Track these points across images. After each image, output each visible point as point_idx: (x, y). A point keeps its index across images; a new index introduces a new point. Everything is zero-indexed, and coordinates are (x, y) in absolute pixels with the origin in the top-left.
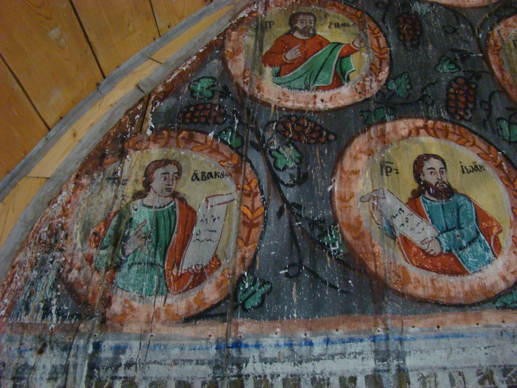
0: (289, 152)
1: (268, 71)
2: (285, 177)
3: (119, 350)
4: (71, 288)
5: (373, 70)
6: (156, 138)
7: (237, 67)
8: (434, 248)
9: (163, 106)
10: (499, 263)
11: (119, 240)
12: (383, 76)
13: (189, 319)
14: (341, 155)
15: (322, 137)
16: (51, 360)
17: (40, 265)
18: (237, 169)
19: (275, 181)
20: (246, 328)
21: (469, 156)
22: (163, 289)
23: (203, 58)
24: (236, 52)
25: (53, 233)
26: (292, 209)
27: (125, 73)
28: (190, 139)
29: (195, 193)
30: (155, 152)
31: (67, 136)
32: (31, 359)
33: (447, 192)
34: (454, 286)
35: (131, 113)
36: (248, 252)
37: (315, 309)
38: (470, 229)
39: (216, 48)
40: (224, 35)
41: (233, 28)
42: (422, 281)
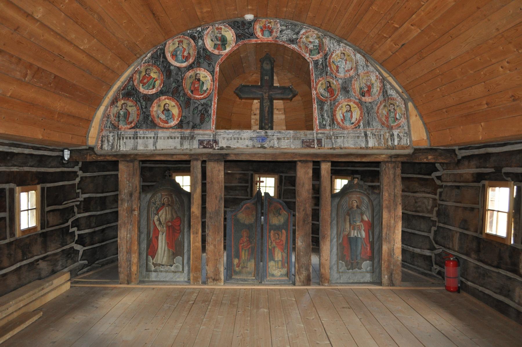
0: (144, 103)
1: (141, 85)
2: (143, 107)
3: (121, 133)
4: (113, 124)
5: (160, 85)
6: (122, 99)
7: (135, 84)
8: (164, 120)
10: (174, 122)
11: (119, 117)
13: (130, 129)
16: (111, 134)
17: (107, 121)
19: (142, 108)
20: (138, 130)
21: (173, 104)
22: (126, 124)
23: (129, 81)
24: (135, 80)
25: (108, 115)
28: (128, 99)
29: (130, 109)
31: (107, 98)
33: (168, 110)
34: (166, 125)
37: (147, 128)
38: (170, 117)
40: (133, 75)
41: (135, 73)
42: (162, 124)
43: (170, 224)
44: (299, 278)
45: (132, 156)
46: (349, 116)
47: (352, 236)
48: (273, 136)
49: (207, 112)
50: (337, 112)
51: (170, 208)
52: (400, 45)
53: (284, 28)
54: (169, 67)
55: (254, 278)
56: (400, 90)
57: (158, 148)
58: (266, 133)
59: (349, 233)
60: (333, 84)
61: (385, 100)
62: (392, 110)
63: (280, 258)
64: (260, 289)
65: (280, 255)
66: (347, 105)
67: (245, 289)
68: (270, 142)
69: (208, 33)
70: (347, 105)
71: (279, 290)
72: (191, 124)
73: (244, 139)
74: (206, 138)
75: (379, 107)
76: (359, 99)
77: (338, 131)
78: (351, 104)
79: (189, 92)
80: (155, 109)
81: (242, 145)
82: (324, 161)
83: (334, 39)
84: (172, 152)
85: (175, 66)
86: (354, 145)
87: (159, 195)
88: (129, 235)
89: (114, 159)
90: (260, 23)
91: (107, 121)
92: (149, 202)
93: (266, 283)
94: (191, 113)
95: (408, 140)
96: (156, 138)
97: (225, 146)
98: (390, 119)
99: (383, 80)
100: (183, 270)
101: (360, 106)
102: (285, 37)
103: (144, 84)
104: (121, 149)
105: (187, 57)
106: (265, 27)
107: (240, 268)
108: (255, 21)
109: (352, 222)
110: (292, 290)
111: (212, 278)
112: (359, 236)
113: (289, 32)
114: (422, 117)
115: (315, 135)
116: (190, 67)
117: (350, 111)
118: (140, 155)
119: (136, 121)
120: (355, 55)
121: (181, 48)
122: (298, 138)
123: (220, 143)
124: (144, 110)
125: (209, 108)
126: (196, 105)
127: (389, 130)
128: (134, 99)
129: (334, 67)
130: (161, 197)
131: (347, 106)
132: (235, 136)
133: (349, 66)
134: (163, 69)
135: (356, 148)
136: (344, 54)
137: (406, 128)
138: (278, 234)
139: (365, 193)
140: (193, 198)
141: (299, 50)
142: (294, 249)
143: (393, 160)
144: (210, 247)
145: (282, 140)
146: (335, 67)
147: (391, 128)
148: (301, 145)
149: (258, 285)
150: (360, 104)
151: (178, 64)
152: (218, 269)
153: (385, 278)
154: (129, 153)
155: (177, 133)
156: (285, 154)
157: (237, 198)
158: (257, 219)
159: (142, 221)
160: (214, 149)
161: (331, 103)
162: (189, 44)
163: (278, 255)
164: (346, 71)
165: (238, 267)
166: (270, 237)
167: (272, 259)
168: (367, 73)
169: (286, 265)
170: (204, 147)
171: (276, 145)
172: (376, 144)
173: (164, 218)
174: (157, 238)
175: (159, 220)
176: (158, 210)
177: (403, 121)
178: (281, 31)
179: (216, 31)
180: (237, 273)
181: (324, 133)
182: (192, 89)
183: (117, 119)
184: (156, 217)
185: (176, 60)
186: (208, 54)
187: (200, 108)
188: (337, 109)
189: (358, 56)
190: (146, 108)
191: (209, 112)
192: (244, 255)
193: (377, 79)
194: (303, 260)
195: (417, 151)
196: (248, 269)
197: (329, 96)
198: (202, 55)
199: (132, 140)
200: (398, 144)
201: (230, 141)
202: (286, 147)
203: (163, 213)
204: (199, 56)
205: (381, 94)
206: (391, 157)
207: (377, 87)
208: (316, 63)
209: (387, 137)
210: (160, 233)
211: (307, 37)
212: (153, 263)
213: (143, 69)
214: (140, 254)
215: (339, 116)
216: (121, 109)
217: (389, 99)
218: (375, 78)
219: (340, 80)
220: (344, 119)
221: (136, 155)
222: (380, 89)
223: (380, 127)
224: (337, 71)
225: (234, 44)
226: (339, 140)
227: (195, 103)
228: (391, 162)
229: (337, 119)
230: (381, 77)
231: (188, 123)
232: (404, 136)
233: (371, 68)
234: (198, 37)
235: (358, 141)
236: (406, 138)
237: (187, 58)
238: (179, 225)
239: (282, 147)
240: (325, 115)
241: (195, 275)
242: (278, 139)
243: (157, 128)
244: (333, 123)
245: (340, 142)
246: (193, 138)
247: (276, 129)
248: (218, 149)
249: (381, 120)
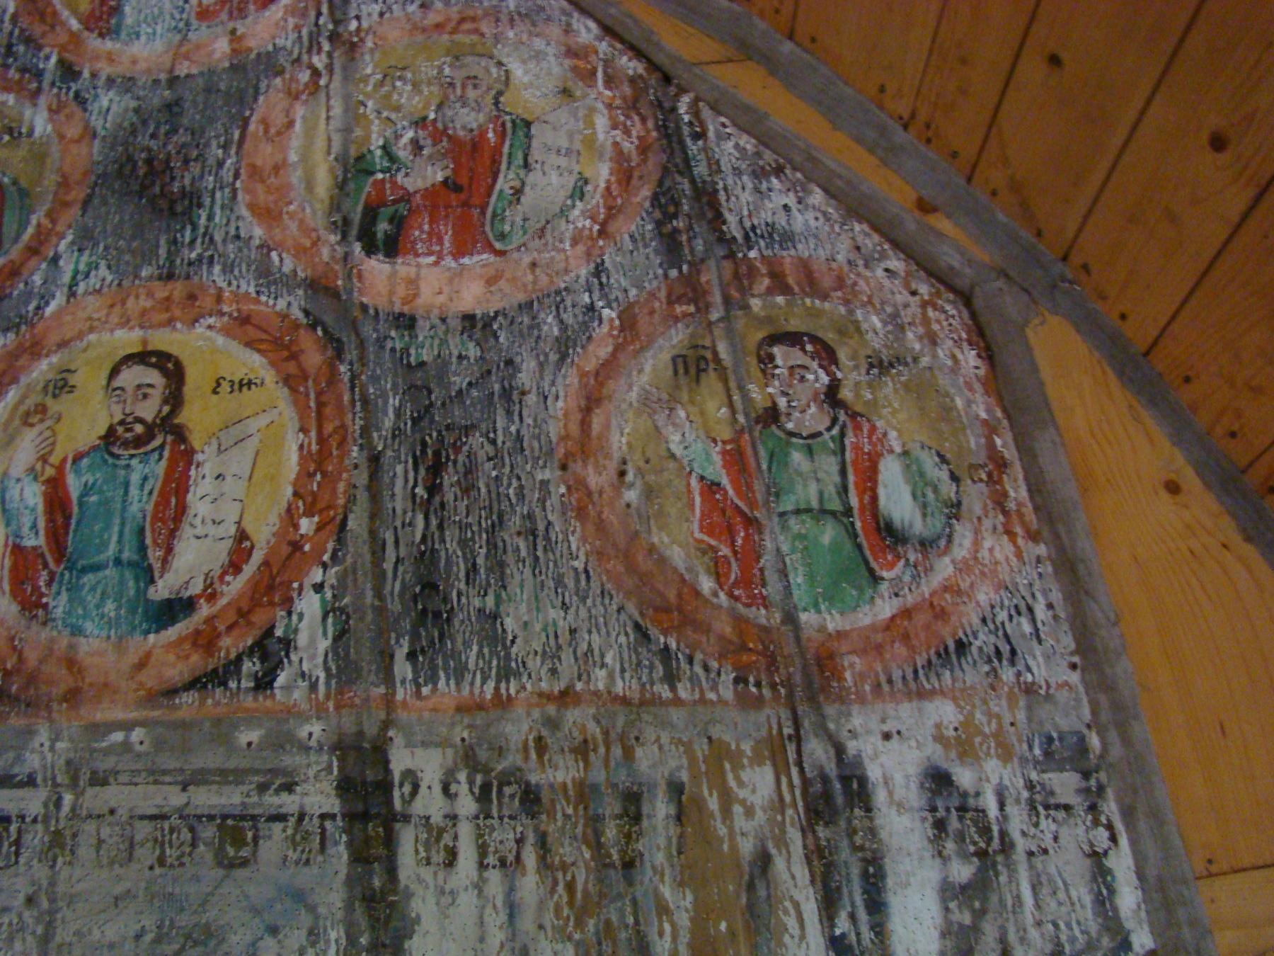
46: (140, 503)
56: (893, 191)
62: (813, 418)
66: (142, 357)
70: (142, 357)
75: (608, 368)
76: (317, 286)
78: (204, 347)
95: (1122, 863)
98: (776, 541)
99: (657, 91)
101: (314, 358)
117: (169, 430)
127: (773, 716)
131: (131, 376)
137: (1050, 664)
147: (801, 680)
150: (326, 340)
177: (988, 564)
205: (635, 223)
207: (574, 151)
209: (744, 833)
217: (743, 277)
218: (555, 68)
222: (625, 175)
223: (613, 673)
230: (630, 65)
232: (1041, 803)
236: (1076, 834)
249: (629, 559)
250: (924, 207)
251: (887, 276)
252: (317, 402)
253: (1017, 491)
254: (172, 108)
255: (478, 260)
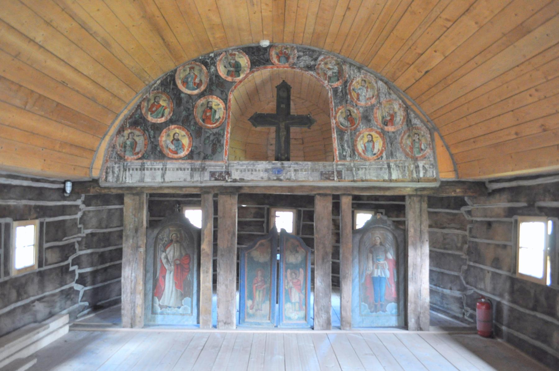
1: (149, 113)
2: (151, 137)
4: (118, 155)
5: (170, 113)
6: (129, 128)
7: (144, 111)
8: (174, 150)
9: (130, 121)
11: (125, 147)
12: (171, 115)
13: (137, 159)
14: (161, 133)
15: (158, 128)
16: (117, 165)
17: (113, 151)
18: (144, 135)
19: (150, 137)
20: (145, 161)
21: (183, 133)
22: (133, 155)
23: (137, 109)
24: (143, 108)
25: (114, 145)
26: (152, 142)
27: (121, 113)
28: (135, 128)
29: (137, 139)
30: (129, 131)
32: (114, 165)
33: (178, 140)
34: (176, 156)
35: (124, 122)
36: (145, 149)
37: (155, 159)
38: (180, 147)
39: (139, 106)
40: (141, 103)
41: (143, 101)
42: (171, 155)
43: (178, 262)
44: (319, 322)
45: (139, 189)
47: (375, 275)
48: (290, 167)
49: (219, 141)
50: (358, 142)
51: (179, 244)
52: (423, 73)
53: (301, 54)
54: (180, 94)
55: (269, 321)
57: (167, 179)
58: (282, 164)
59: (372, 273)
60: (354, 112)
61: (409, 129)
62: (417, 140)
63: (297, 300)
64: (275, 334)
65: (297, 295)
67: (259, 334)
68: (286, 174)
69: (221, 59)
71: (296, 334)
72: (202, 155)
73: (259, 171)
74: (218, 169)
76: (382, 129)
77: (359, 163)
78: (373, 133)
79: (201, 121)
80: (164, 139)
81: (257, 177)
82: (344, 194)
83: (355, 66)
84: (182, 184)
85: (186, 94)
86: (377, 177)
87: (167, 230)
88: (133, 274)
89: (120, 192)
90: (276, 49)
91: (113, 151)
92: (157, 238)
93: (282, 327)
94: (202, 142)
95: (434, 172)
96: (164, 170)
97: (238, 178)
98: (414, 150)
99: (407, 109)
100: (192, 312)
102: (302, 63)
103: (152, 112)
104: (127, 181)
105: (198, 84)
106: (281, 52)
107: (254, 310)
108: (270, 47)
109: (375, 260)
110: (311, 334)
111: (223, 321)
112: (383, 276)
113: (306, 58)
114: (448, 148)
115: (335, 167)
116: (202, 95)
118: (147, 188)
119: (143, 151)
120: (376, 83)
121: (192, 74)
122: (316, 170)
123: (233, 175)
124: (152, 140)
125: (221, 138)
126: (208, 135)
128: (142, 128)
129: (354, 95)
130: (169, 234)
131: (369, 136)
132: (249, 167)
133: (370, 93)
134: (173, 97)
135: (378, 181)
136: (365, 81)
137: (432, 159)
138: (296, 274)
139: (389, 228)
140: (204, 234)
141: (317, 77)
142: (313, 289)
143: (419, 193)
144: (220, 287)
145: (300, 172)
146: (356, 95)
147: (415, 159)
148: (320, 177)
149: (273, 329)
150: (383, 134)
151: (189, 92)
152: (230, 311)
153: (412, 322)
154: (135, 185)
155: (187, 164)
156: (302, 187)
157: (253, 235)
158: (273, 256)
159: (148, 259)
160: (227, 181)
161: (351, 133)
162: (201, 70)
163: (296, 296)
164: (367, 99)
165: (252, 308)
166: (286, 276)
167: (289, 300)
168: (390, 102)
169: (304, 307)
170: (216, 179)
171: (293, 177)
172: (400, 176)
173: (172, 256)
174: (164, 277)
175: (166, 258)
176: (165, 247)
177: (428, 152)
178: (298, 58)
179: (230, 57)
180: (250, 316)
181: (344, 165)
182: (204, 117)
183: (123, 149)
184: (163, 255)
185: (188, 88)
186: (221, 80)
187: (212, 138)
188: (359, 139)
189: (380, 83)
190: (154, 137)
191: (222, 142)
192: (258, 296)
193: (400, 107)
194: (323, 302)
195: (445, 184)
196: (263, 312)
197: (349, 125)
198: (214, 82)
199: (139, 172)
200: (424, 176)
201: (244, 173)
202: (304, 179)
203: (170, 251)
204: (211, 83)
205: (405, 123)
206: (416, 190)
207: (400, 116)
208: (335, 90)
209: (411, 169)
210: (168, 272)
211: (326, 64)
212: (160, 305)
213: (151, 96)
214: (145, 295)
215: (360, 147)
216: (127, 139)
219: (361, 109)
220: (366, 150)
221: (143, 187)
222: (404, 118)
223: (404, 159)
224: (358, 99)
225: (248, 71)
226: (361, 172)
227: (207, 132)
228: (416, 196)
229: (358, 150)
230: (404, 106)
231: (199, 154)
232: (430, 168)
233: (394, 96)
234: (211, 64)
235: (381, 173)
236: (432, 170)
237: (198, 86)
238: (189, 264)
239: (300, 179)
240: (346, 145)
241: (204, 318)
242: (295, 170)
243: (165, 159)
244: (354, 153)
245: (361, 174)
246: (203, 169)
247: (293, 160)
248: (231, 182)
250: (428, 122)
251: (424, 128)
252: (383, 139)
253: (431, 146)
254: (367, 110)
255: (393, 127)
